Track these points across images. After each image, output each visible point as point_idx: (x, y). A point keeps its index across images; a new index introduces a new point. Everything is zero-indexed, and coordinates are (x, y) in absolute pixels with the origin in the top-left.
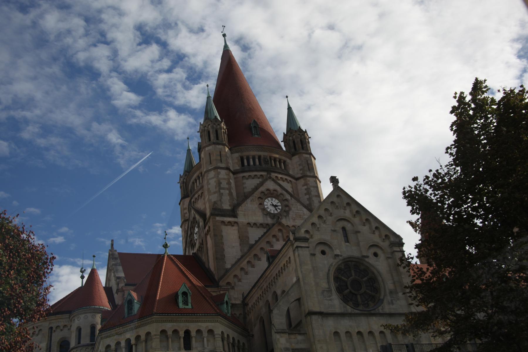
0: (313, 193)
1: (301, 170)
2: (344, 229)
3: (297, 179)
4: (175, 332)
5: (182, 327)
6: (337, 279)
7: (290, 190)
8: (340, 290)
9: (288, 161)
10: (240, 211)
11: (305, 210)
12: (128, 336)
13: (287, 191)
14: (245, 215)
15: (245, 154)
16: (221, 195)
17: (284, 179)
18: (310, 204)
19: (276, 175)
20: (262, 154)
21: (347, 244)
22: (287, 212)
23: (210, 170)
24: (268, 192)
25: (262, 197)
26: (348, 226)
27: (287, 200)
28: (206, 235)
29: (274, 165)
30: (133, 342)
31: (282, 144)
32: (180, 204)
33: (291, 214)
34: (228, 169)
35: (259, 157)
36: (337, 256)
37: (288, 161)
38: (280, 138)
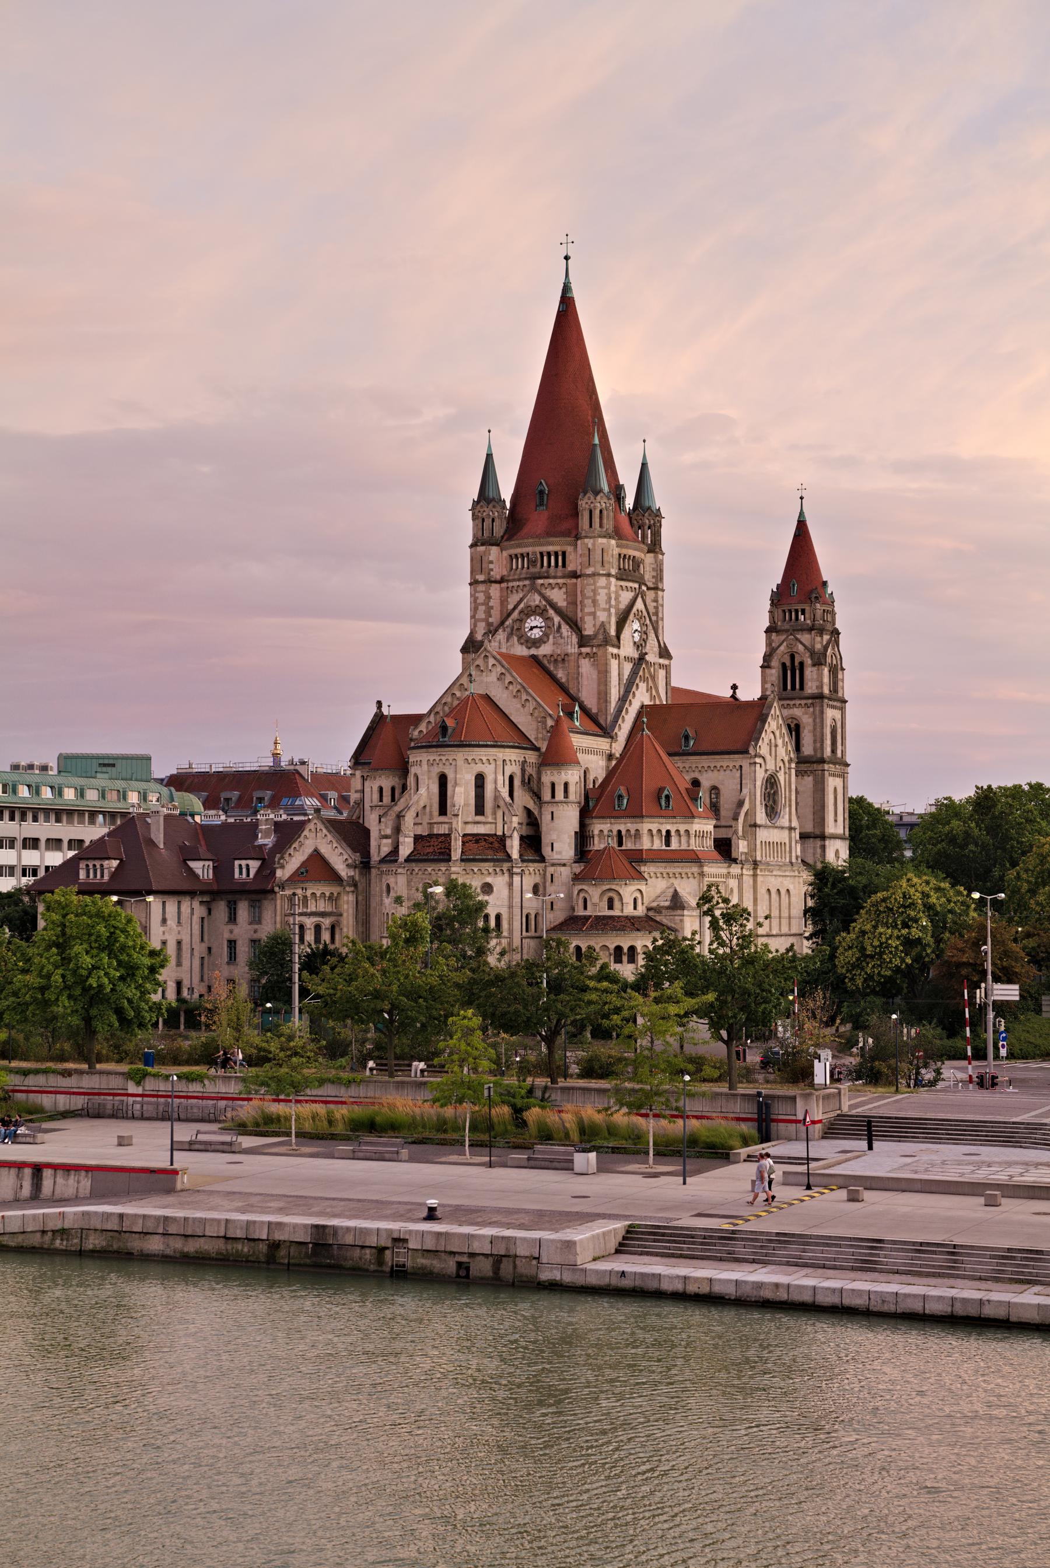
0: (660, 615)
1: (653, 577)
3: (648, 589)
12: (668, 827)
15: (624, 551)
16: (610, 615)
30: (673, 833)
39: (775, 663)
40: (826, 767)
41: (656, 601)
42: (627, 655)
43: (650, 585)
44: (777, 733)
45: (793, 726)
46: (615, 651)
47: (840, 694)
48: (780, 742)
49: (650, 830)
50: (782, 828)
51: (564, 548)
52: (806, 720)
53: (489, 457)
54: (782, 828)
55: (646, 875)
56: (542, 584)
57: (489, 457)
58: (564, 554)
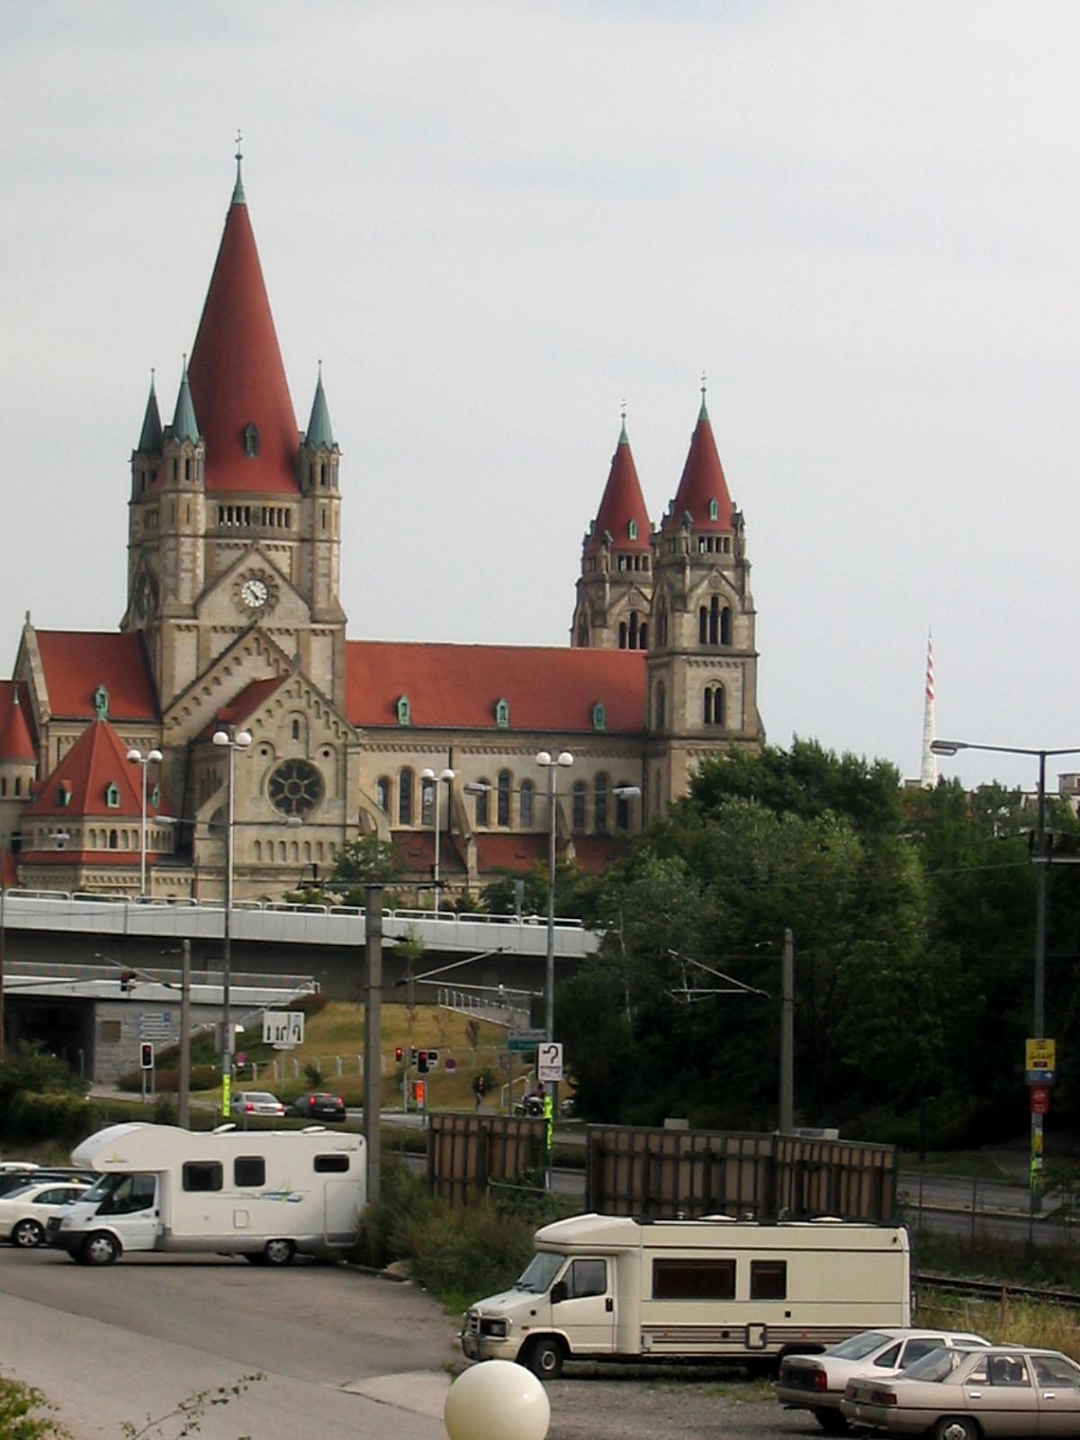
0: (321, 568)
2: (296, 722)
4: (103, 831)
5: (109, 826)
6: (273, 782)
8: (273, 795)
10: (204, 609)
11: (301, 604)
14: (209, 615)
15: (228, 503)
18: (311, 590)
19: (268, 542)
21: (295, 741)
22: (272, 607)
26: (301, 719)
27: (276, 586)
33: (279, 609)
35: (248, 509)
36: (275, 758)
39: (654, 611)
40: (675, 743)
41: (312, 554)
42: (218, 622)
43: (308, 536)
44: (311, 713)
45: (714, 690)
47: (740, 644)
48: (318, 724)
49: (41, 831)
50: (323, 825)
52: (667, 683)
53: (152, 400)
54: (323, 825)
55: (21, 879)
57: (152, 400)
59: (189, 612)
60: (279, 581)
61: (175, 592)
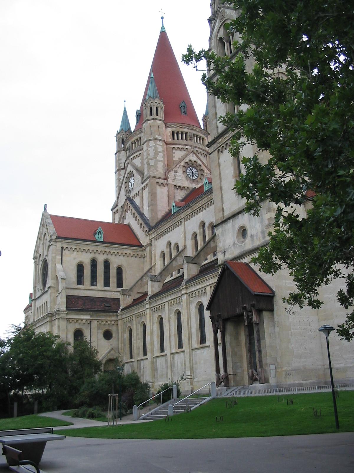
7: (205, 162)
9: (205, 138)
13: (203, 163)
17: (202, 153)
19: (197, 149)
20: (188, 131)
23: (151, 140)
24: (191, 162)
25: (186, 166)
28: (143, 189)
29: (196, 141)
31: (201, 123)
32: (116, 154)
34: (165, 142)
37: (205, 138)
38: (200, 117)
46: (161, 181)
51: (139, 136)
53: (125, 111)
56: (132, 158)
58: (140, 138)
59: (164, 177)
60: (203, 167)
61: (155, 166)
